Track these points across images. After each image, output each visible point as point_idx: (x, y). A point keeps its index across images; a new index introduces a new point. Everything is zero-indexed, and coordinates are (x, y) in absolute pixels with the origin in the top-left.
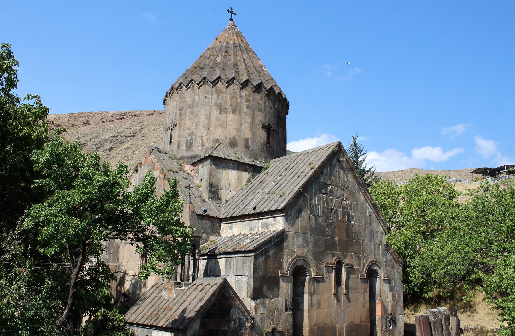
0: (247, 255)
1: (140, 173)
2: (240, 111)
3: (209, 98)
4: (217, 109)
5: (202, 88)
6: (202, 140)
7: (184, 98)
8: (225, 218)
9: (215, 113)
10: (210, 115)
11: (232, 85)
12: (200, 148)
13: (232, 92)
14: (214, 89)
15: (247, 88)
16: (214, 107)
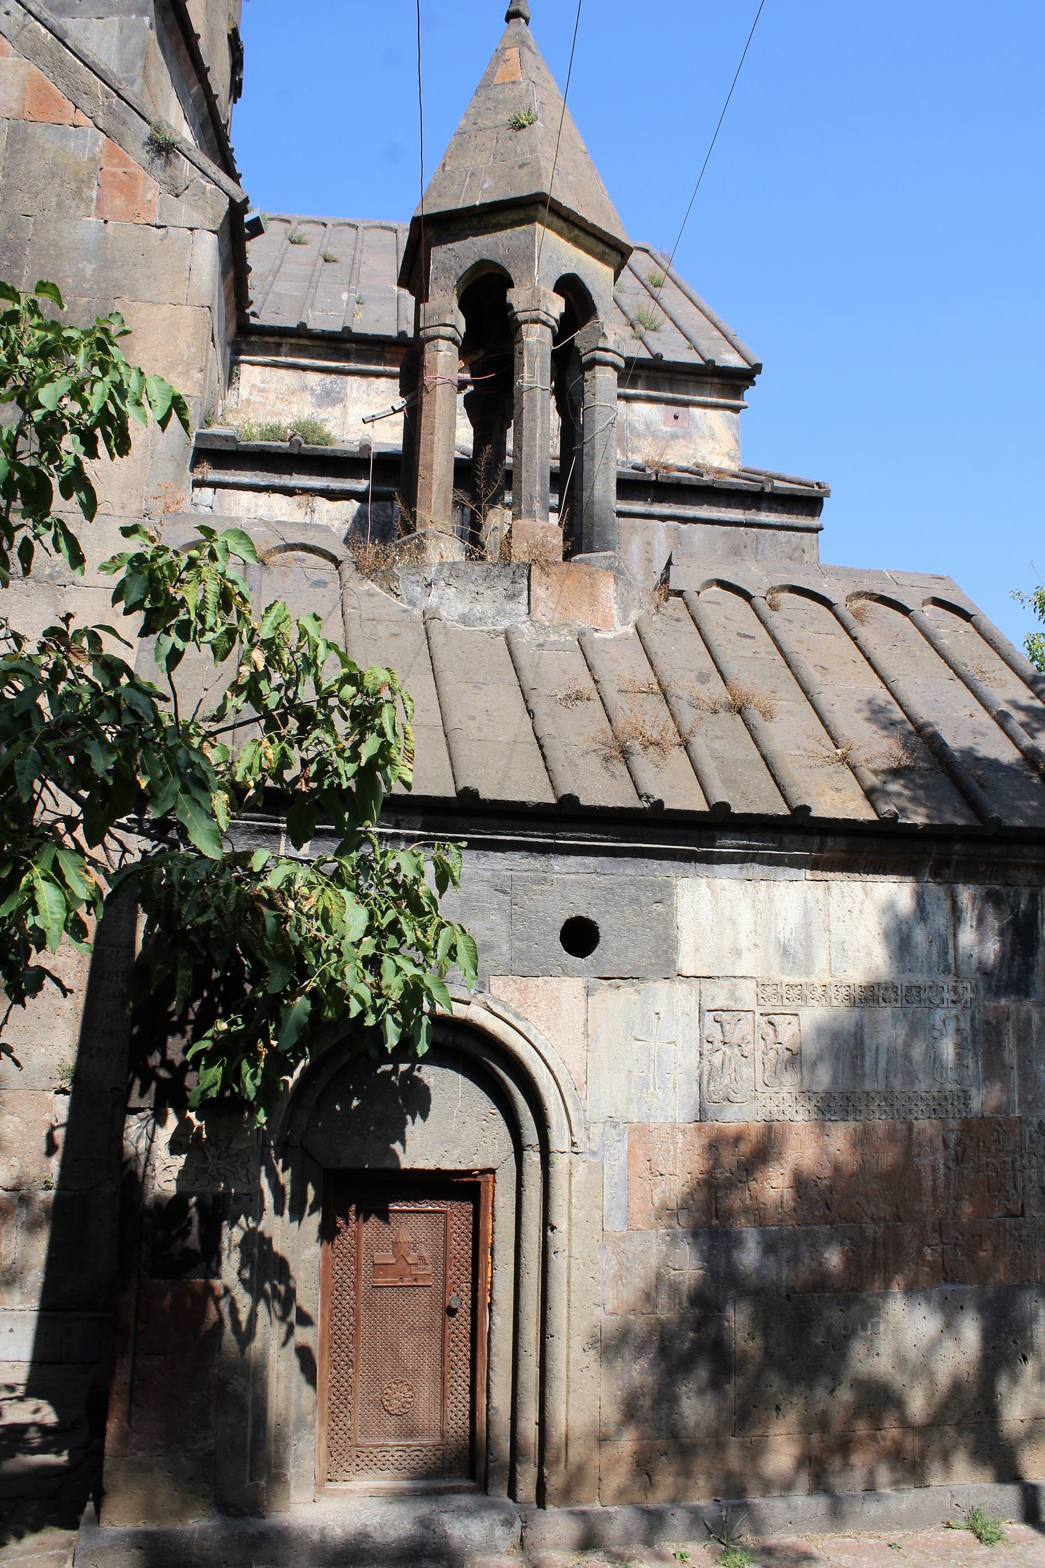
0: (765, 517)
8: (301, 332)
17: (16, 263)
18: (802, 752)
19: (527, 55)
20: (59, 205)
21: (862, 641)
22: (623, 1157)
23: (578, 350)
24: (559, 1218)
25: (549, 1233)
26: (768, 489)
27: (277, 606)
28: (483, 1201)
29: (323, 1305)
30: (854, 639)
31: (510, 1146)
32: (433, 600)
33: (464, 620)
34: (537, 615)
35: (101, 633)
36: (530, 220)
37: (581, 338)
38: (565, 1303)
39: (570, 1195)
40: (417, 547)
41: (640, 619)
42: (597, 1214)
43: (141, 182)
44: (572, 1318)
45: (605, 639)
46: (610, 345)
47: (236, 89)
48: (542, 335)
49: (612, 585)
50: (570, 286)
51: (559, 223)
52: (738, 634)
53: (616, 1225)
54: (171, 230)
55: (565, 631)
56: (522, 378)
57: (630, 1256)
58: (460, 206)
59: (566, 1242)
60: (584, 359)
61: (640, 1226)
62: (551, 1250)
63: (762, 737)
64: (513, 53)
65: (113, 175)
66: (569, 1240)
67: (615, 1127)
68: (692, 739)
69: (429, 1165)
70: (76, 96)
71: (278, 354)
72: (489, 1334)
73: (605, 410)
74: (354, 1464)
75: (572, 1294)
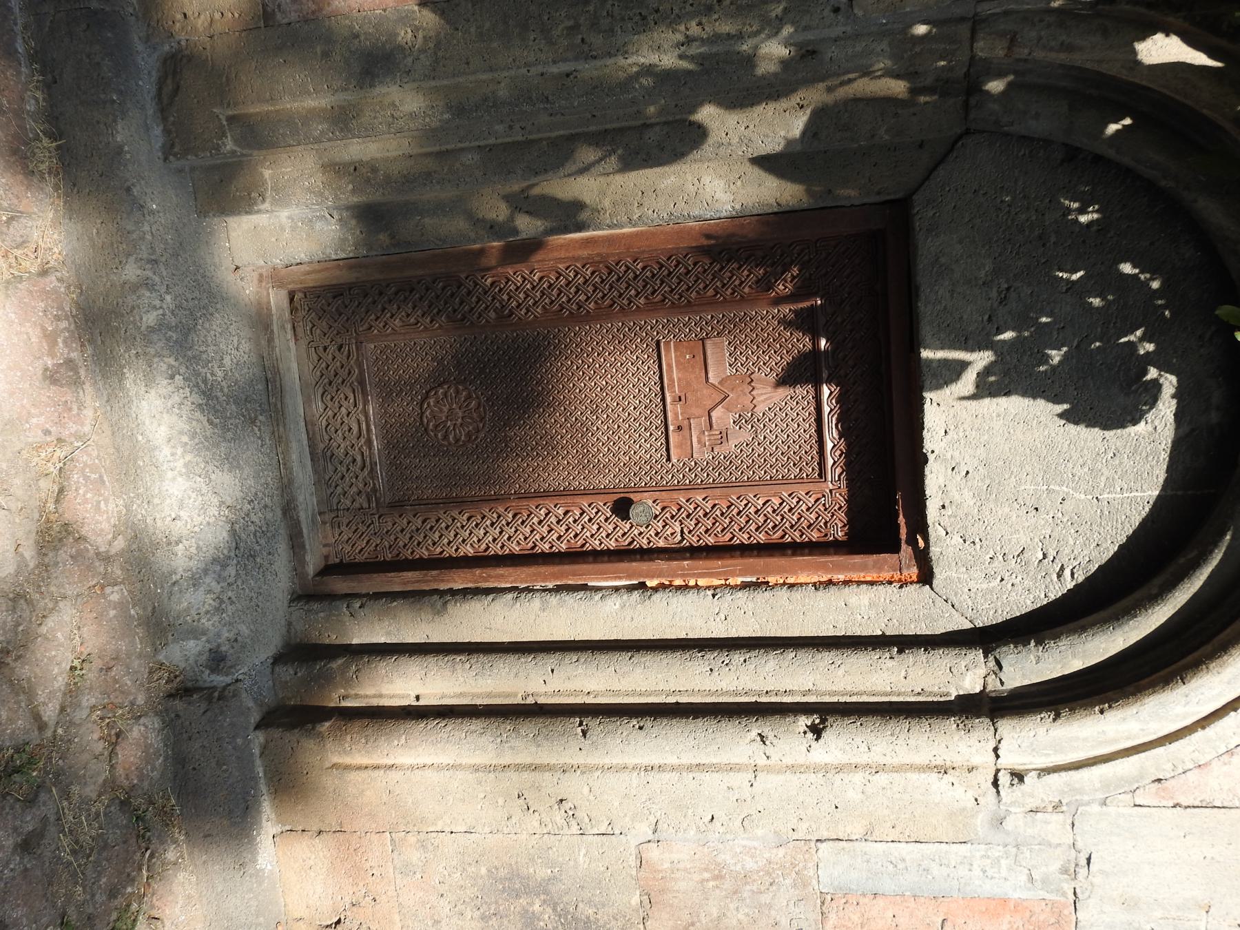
22: (989, 888)
24: (842, 742)
25: (804, 721)
28: (858, 559)
29: (610, 240)
31: (988, 617)
38: (655, 760)
39: (897, 769)
42: (857, 830)
44: (624, 776)
53: (834, 869)
57: (765, 898)
59: (788, 761)
61: (832, 919)
62: (765, 726)
66: (792, 768)
67: (1065, 871)
69: (932, 441)
72: (584, 587)
74: (327, 342)
75: (674, 776)
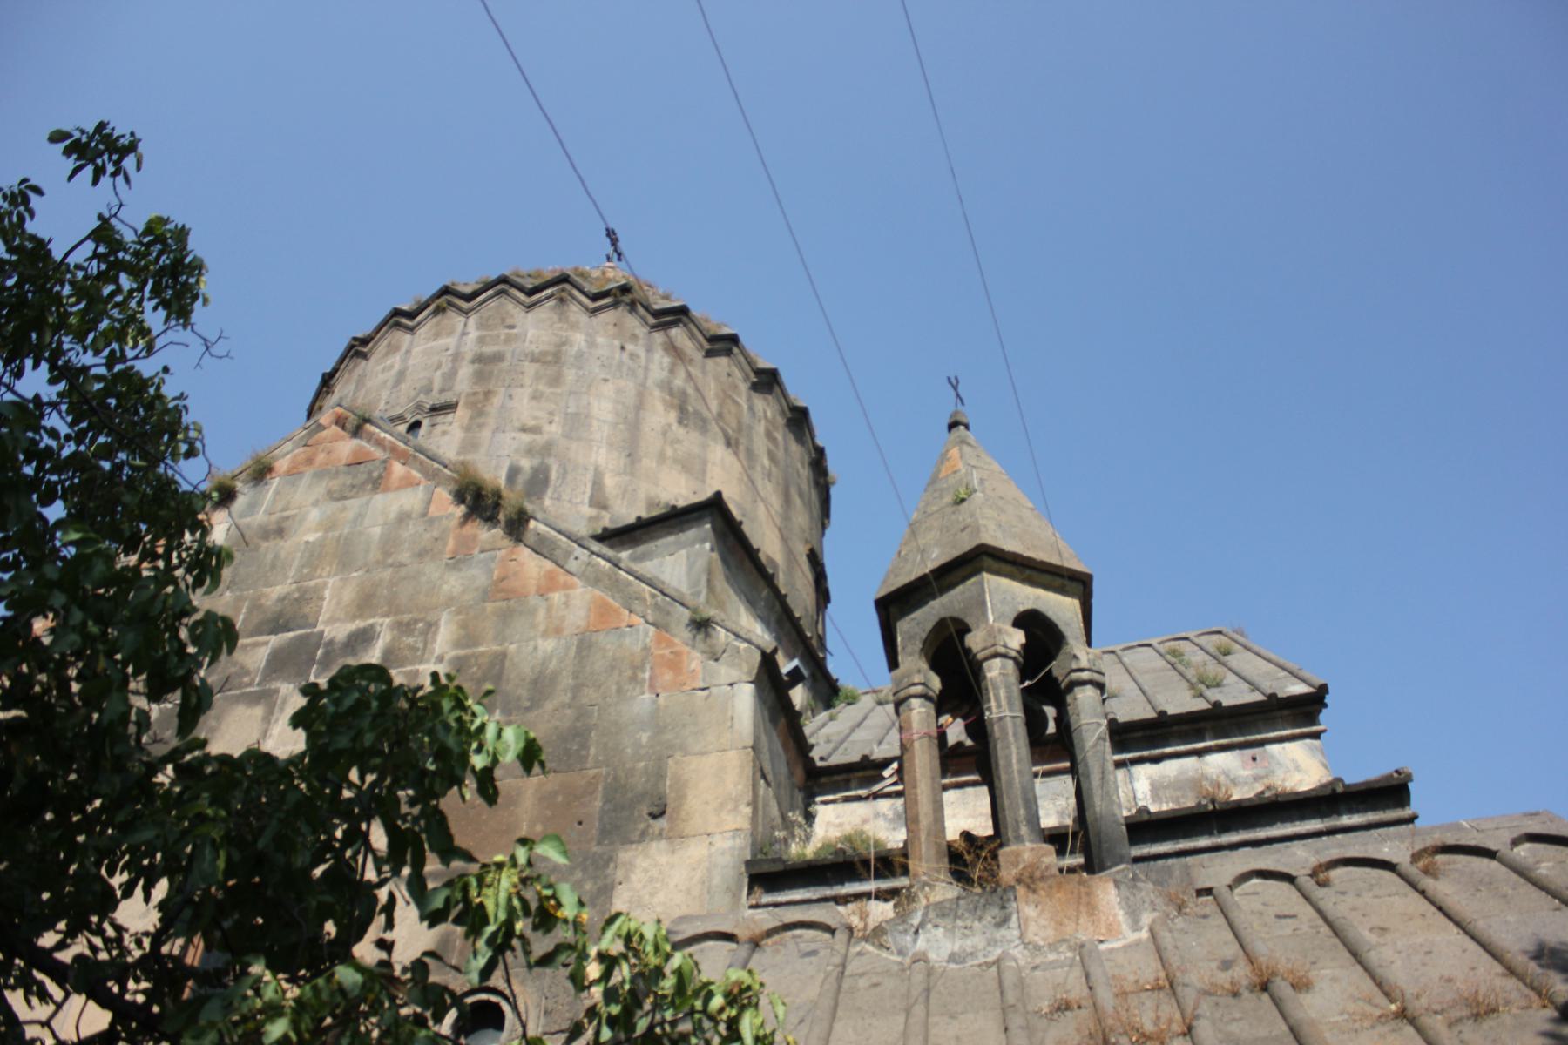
0: (1346, 820)
1: (252, 507)
2: (750, 454)
3: (633, 356)
4: (668, 406)
5: (608, 316)
6: (597, 484)
7: (512, 327)
9: (659, 416)
10: (640, 406)
11: (723, 361)
12: (588, 511)
13: (724, 378)
14: (659, 337)
15: (770, 397)
16: (657, 393)
17: (584, 746)
18: (1346, 1016)
19: (966, 449)
20: (619, 691)
21: (1430, 893)
23: (1056, 680)
26: (1340, 789)
27: (622, 918)
30: (1422, 893)
32: (921, 944)
33: (952, 958)
34: (1030, 936)
35: (427, 960)
36: (977, 572)
37: (1058, 668)
40: (908, 897)
41: (1154, 921)
43: (685, 657)
45: (1111, 951)
46: (1084, 663)
47: (823, 595)
48: (1003, 667)
49: (1113, 891)
50: (1030, 621)
51: (1008, 568)
52: (1278, 917)
54: (714, 690)
55: (1064, 947)
56: (989, 709)
58: (913, 578)
60: (1063, 686)
63: (1289, 1007)
64: (955, 452)
65: (662, 656)
68: (1195, 1023)
70: (630, 602)
71: (848, 789)
73: (1092, 727)
